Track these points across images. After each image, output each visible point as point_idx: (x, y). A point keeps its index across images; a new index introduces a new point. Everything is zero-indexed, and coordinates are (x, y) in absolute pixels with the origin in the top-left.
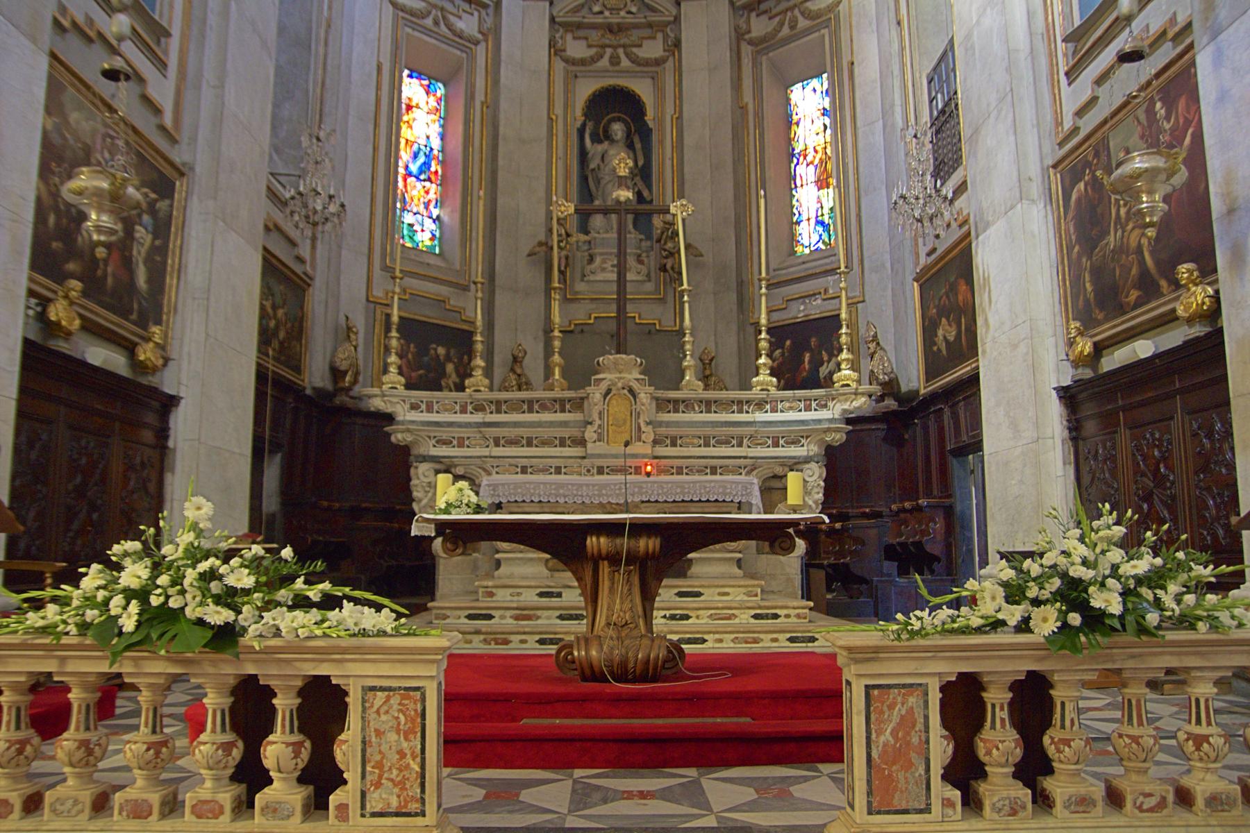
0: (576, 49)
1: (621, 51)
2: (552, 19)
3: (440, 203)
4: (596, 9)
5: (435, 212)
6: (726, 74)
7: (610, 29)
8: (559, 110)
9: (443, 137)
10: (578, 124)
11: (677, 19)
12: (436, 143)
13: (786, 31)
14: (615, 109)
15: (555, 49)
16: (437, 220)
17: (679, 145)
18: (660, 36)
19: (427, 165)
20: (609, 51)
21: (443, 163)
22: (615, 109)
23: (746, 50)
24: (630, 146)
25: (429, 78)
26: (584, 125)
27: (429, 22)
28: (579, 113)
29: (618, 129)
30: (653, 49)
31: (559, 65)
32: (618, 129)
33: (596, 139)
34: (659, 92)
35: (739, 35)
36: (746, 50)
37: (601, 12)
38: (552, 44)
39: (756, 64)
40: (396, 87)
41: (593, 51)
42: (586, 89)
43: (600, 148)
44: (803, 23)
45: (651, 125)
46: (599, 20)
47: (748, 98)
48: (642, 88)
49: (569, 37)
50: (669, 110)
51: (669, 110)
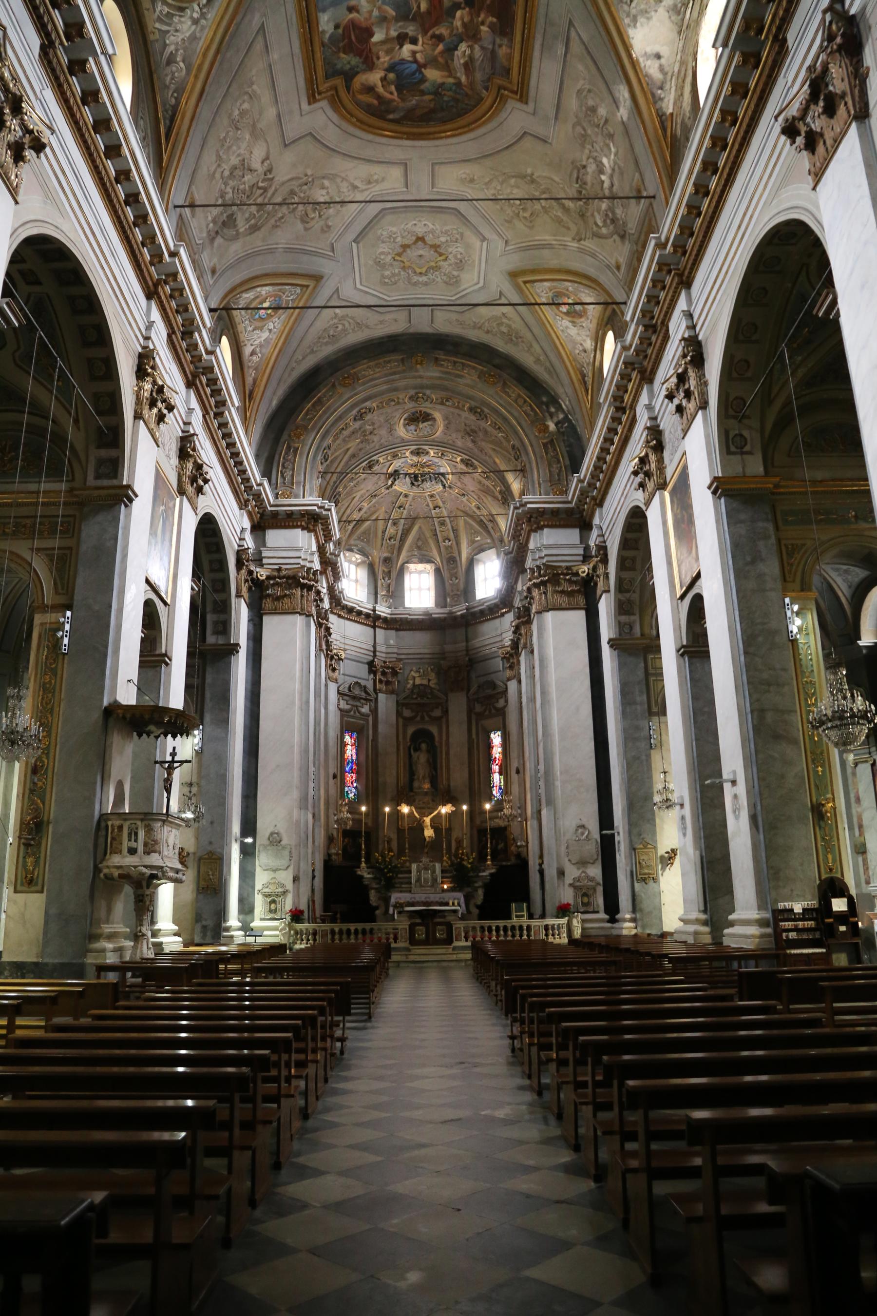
0: (407, 713)
1: (425, 714)
2: (397, 701)
5: (355, 785)
6: (465, 726)
9: (357, 754)
11: (447, 701)
12: (354, 757)
13: (487, 713)
14: (421, 738)
15: (399, 714)
16: (356, 788)
17: (448, 754)
19: (352, 767)
20: (420, 714)
21: (357, 765)
22: (421, 738)
23: (474, 717)
24: (428, 751)
27: (352, 713)
28: (408, 740)
30: (437, 713)
31: (401, 720)
33: (416, 750)
35: (470, 711)
36: (474, 717)
38: (397, 711)
39: (477, 724)
40: (342, 738)
42: (411, 730)
43: (417, 754)
44: (493, 711)
45: (437, 744)
46: (415, 701)
47: (474, 736)
48: (434, 730)
50: (444, 738)
51: (444, 738)
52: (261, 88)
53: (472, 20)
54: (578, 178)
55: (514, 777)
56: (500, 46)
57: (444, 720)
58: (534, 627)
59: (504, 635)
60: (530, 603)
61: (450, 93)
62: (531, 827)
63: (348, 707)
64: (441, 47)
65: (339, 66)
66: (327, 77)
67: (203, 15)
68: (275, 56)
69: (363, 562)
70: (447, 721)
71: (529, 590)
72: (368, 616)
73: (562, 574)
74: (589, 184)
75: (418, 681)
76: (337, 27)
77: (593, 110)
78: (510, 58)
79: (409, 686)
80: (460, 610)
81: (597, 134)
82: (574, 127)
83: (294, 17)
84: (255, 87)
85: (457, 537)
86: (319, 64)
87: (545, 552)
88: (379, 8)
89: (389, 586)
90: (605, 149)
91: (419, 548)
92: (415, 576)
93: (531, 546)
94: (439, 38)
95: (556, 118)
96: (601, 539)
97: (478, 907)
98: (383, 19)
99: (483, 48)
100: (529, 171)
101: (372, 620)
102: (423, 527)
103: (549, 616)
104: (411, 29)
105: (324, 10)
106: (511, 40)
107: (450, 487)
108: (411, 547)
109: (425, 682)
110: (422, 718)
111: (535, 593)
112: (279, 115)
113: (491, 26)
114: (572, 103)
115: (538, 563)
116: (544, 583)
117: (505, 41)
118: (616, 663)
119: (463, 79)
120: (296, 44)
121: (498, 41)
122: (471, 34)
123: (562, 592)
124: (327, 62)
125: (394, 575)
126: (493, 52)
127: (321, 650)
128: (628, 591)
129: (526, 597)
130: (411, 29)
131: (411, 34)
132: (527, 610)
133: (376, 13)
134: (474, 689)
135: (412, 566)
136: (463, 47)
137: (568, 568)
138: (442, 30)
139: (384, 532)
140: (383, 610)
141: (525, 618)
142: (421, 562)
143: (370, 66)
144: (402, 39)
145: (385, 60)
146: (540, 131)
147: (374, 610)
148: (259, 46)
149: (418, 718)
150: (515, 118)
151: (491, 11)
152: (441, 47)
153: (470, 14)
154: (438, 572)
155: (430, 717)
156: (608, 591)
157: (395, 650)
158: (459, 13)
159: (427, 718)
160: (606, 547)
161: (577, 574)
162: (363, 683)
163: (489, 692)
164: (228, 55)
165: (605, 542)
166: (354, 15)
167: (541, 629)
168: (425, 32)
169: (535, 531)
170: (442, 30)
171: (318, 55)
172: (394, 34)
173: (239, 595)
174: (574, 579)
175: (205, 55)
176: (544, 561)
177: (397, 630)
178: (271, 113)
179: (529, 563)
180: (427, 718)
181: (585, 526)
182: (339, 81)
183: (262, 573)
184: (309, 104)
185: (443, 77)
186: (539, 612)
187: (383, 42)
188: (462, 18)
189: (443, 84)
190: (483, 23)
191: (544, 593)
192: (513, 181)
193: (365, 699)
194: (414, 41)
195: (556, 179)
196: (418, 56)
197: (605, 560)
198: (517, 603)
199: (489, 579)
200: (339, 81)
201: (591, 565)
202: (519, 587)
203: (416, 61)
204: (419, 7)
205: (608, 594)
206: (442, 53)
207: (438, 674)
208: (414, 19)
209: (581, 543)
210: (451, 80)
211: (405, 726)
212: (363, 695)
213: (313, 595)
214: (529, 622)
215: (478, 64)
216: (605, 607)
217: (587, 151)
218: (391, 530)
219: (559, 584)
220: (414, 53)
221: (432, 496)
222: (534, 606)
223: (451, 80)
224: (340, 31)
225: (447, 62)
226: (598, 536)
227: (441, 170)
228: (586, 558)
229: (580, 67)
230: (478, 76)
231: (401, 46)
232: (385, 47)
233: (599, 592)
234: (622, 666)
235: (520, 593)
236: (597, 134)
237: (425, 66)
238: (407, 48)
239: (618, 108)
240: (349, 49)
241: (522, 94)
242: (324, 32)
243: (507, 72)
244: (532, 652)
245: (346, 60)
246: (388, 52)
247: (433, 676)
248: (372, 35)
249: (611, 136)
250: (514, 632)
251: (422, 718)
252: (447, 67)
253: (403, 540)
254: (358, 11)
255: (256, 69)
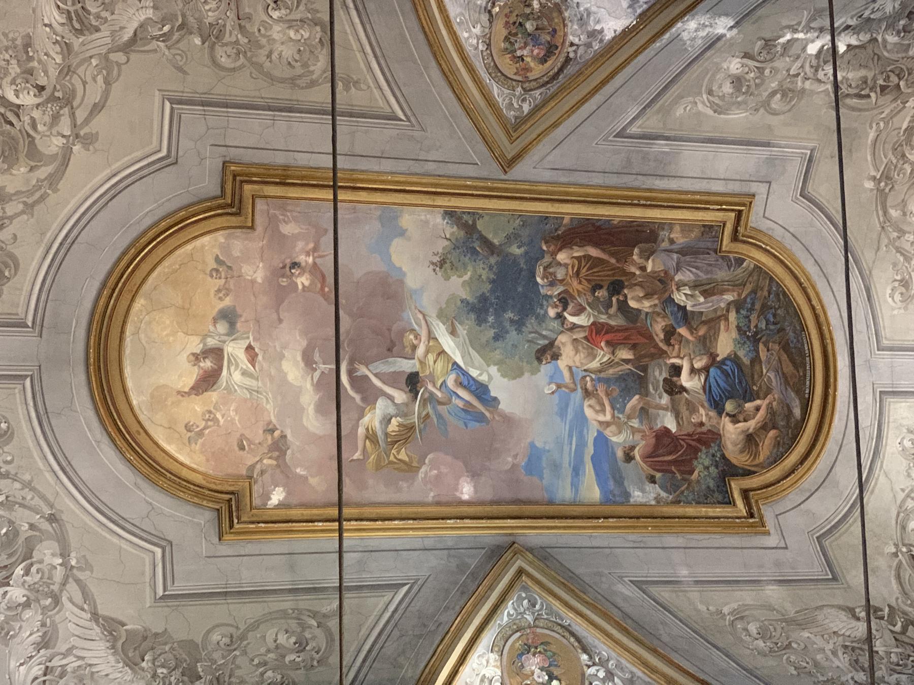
52: (729, 602)
53: (640, 285)
54: (859, 96)
56: (672, 241)
61: (754, 317)
64: (683, 331)
65: (712, 484)
66: (730, 502)
67: (603, 663)
68: (684, 573)
74: (863, 73)
76: (652, 480)
77: (737, 81)
78: (687, 227)
81: (774, 70)
82: (775, 113)
83: (632, 537)
84: (726, 610)
86: (704, 510)
88: (629, 418)
90: (795, 50)
94: (670, 333)
95: (768, 144)
98: (644, 412)
99: (678, 269)
100: (869, 185)
104: (659, 374)
105: (627, 495)
106: (662, 225)
112: (780, 582)
113: (648, 254)
114: (738, 119)
117: (663, 234)
119: (729, 297)
120: (671, 540)
121: (665, 245)
122: (660, 285)
124: (704, 499)
126: (683, 252)
130: (659, 374)
131: (665, 375)
133: (635, 423)
136: (679, 298)
138: (658, 328)
143: (712, 438)
144: (673, 388)
145: (704, 415)
146: (795, 169)
148: (664, 594)
150: (780, 214)
151: (625, 257)
152: (683, 331)
153: (631, 286)
158: (632, 304)
164: (665, 638)
166: (637, 453)
168: (662, 354)
170: (658, 328)
171: (690, 511)
172: (665, 400)
175: (653, 670)
178: (773, 593)
182: (736, 486)
184: (768, 533)
185: (727, 329)
187: (677, 416)
188: (639, 299)
189: (739, 328)
190: (643, 269)
192: (894, 213)
194: (676, 370)
195: (872, 135)
196: (698, 365)
200: (736, 486)
203: (706, 369)
204: (627, 361)
206: (691, 330)
208: (645, 369)
210: (732, 316)
215: (703, 276)
217: (808, 84)
220: (693, 371)
223: (732, 316)
224: (658, 475)
225: (704, 323)
227: (889, 335)
229: (679, 111)
230: (721, 274)
231: (684, 389)
232: (685, 413)
236: (774, 70)
237: (713, 356)
238: (685, 380)
239: (720, 38)
240: (685, 465)
241: (740, 206)
242: (658, 500)
243: (710, 230)
245: (703, 470)
246: (692, 409)
248: (667, 431)
249: (769, 44)
252: (714, 322)
254: (632, 448)
255: (698, 603)
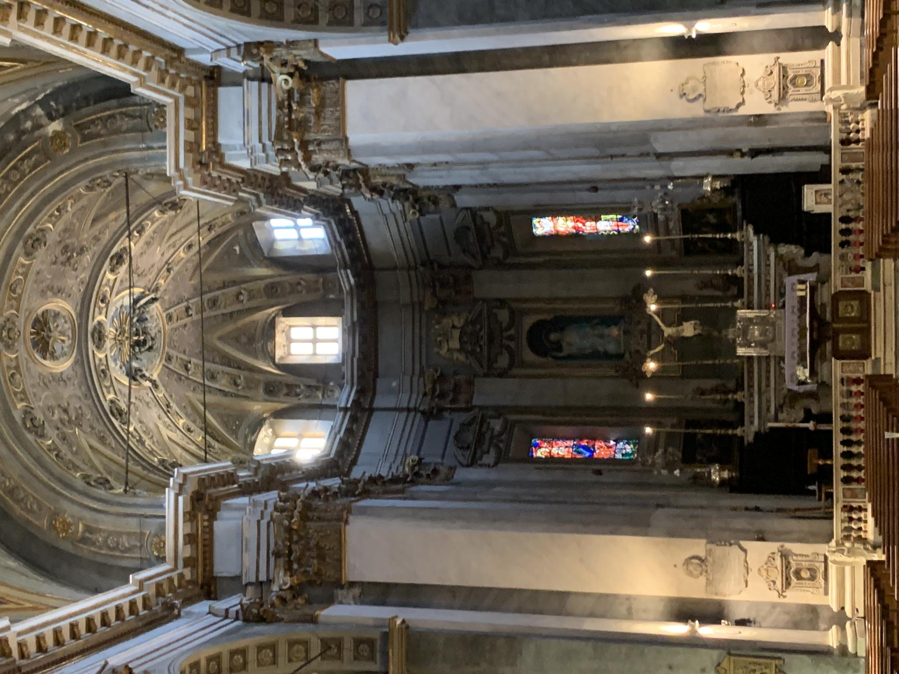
0: (503, 361)
1: (505, 334)
2: (486, 375)
3: (606, 440)
4: (478, 350)
5: (612, 443)
7: (491, 341)
8: (541, 371)
10: (550, 359)
11: (484, 300)
12: (570, 443)
15: (503, 374)
17: (566, 300)
18: (494, 311)
21: (581, 439)
23: (510, 260)
24: (562, 329)
25: (531, 446)
26: (553, 357)
27: (501, 445)
28: (544, 360)
29: (553, 337)
30: (504, 315)
31: (515, 371)
32: (553, 337)
33: (560, 348)
34: (528, 312)
35: (500, 265)
36: (510, 260)
37: (481, 346)
38: (500, 376)
41: (504, 351)
42: (529, 356)
45: (551, 317)
46: (485, 348)
47: (541, 259)
48: (528, 322)
49: (496, 365)
55: (601, 197)
57: (514, 305)
58: (372, 161)
59: (386, 210)
60: (336, 168)
62: (679, 167)
63: (493, 452)
69: (272, 426)
70: (517, 300)
71: (314, 169)
72: (354, 419)
73: (289, 115)
75: (455, 344)
79: (462, 357)
80: (347, 279)
85: (234, 283)
87: (255, 141)
89: (309, 387)
91: (251, 340)
92: (295, 349)
93: (245, 164)
96: (234, 52)
97: (808, 254)
101: (360, 415)
102: (219, 333)
103: (356, 136)
107: (157, 290)
108: (248, 353)
109: (456, 334)
110: (511, 338)
111: (319, 159)
115: (272, 153)
116: (304, 145)
118: (429, 32)
123: (318, 114)
125: (291, 379)
127: (402, 491)
128: (315, 9)
129: (326, 173)
132: (346, 174)
134: (470, 261)
135: (279, 353)
137: (280, 106)
139: (225, 394)
140: (344, 397)
141: (358, 177)
142: (273, 337)
147: (345, 410)
149: (512, 344)
154: (288, 312)
155: (509, 328)
156: (316, 42)
157: (408, 378)
159: (512, 332)
160: (247, 44)
161: (290, 92)
162: (455, 428)
163: (472, 237)
165: (238, 46)
167: (374, 150)
169: (222, 156)
173: (313, 620)
174: (296, 96)
176: (268, 143)
177: (376, 375)
179: (273, 169)
180: (512, 332)
181: (214, 77)
183: (283, 580)
186: (349, 153)
191: (319, 144)
193: (481, 426)
197: (269, 45)
198: (335, 189)
199: (298, 234)
201: (276, 69)
202: (311, 186)
205: (320, 43)
207: (445, 315)
209: (240, 84)
211: (523, 364)
212: (475, 427)
213: (318, 503)
214: (364, 171)
216: (340, 48)
218: (223, 383)
219: (306, 120)
221: (170, 318)
222: (340, 161)
226: (229, 56)
228: (264, 78)
233: (317, 58)
234: (433, 23)
235: (320, 184)
244: (410, 166)
247: (447, 322)
250: (381, 194)
251: (511, 338)
253: (240, 366)
